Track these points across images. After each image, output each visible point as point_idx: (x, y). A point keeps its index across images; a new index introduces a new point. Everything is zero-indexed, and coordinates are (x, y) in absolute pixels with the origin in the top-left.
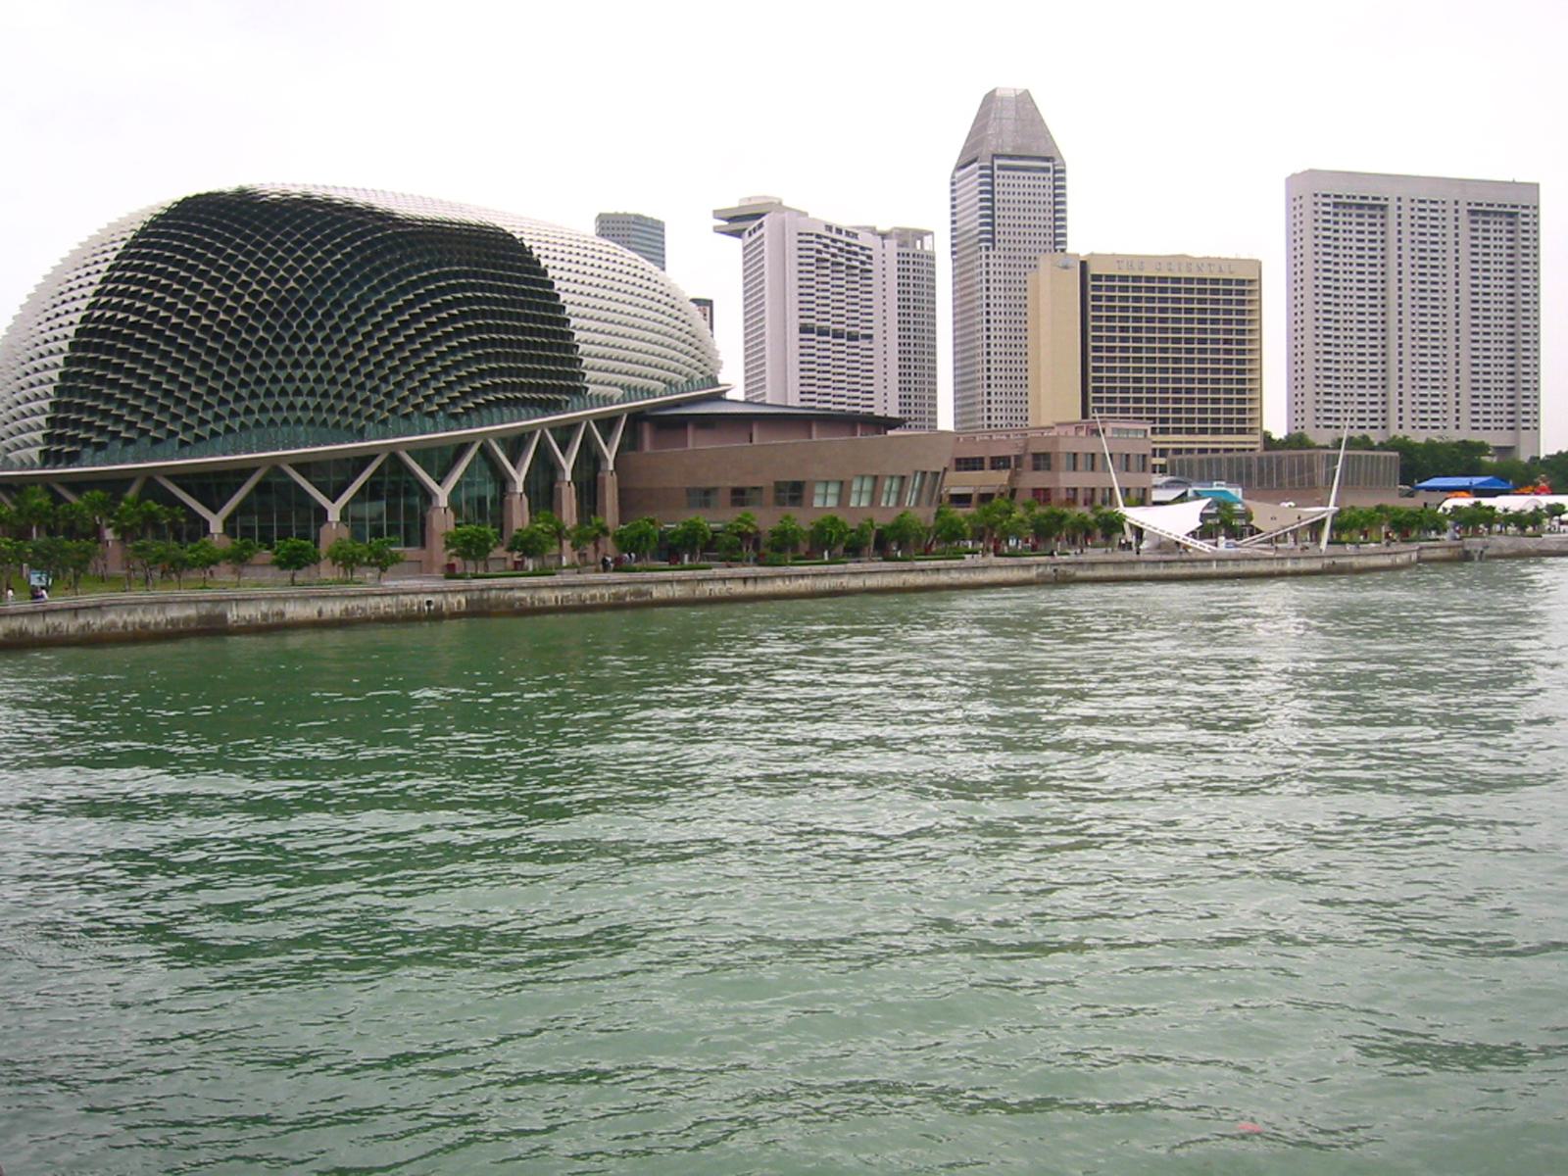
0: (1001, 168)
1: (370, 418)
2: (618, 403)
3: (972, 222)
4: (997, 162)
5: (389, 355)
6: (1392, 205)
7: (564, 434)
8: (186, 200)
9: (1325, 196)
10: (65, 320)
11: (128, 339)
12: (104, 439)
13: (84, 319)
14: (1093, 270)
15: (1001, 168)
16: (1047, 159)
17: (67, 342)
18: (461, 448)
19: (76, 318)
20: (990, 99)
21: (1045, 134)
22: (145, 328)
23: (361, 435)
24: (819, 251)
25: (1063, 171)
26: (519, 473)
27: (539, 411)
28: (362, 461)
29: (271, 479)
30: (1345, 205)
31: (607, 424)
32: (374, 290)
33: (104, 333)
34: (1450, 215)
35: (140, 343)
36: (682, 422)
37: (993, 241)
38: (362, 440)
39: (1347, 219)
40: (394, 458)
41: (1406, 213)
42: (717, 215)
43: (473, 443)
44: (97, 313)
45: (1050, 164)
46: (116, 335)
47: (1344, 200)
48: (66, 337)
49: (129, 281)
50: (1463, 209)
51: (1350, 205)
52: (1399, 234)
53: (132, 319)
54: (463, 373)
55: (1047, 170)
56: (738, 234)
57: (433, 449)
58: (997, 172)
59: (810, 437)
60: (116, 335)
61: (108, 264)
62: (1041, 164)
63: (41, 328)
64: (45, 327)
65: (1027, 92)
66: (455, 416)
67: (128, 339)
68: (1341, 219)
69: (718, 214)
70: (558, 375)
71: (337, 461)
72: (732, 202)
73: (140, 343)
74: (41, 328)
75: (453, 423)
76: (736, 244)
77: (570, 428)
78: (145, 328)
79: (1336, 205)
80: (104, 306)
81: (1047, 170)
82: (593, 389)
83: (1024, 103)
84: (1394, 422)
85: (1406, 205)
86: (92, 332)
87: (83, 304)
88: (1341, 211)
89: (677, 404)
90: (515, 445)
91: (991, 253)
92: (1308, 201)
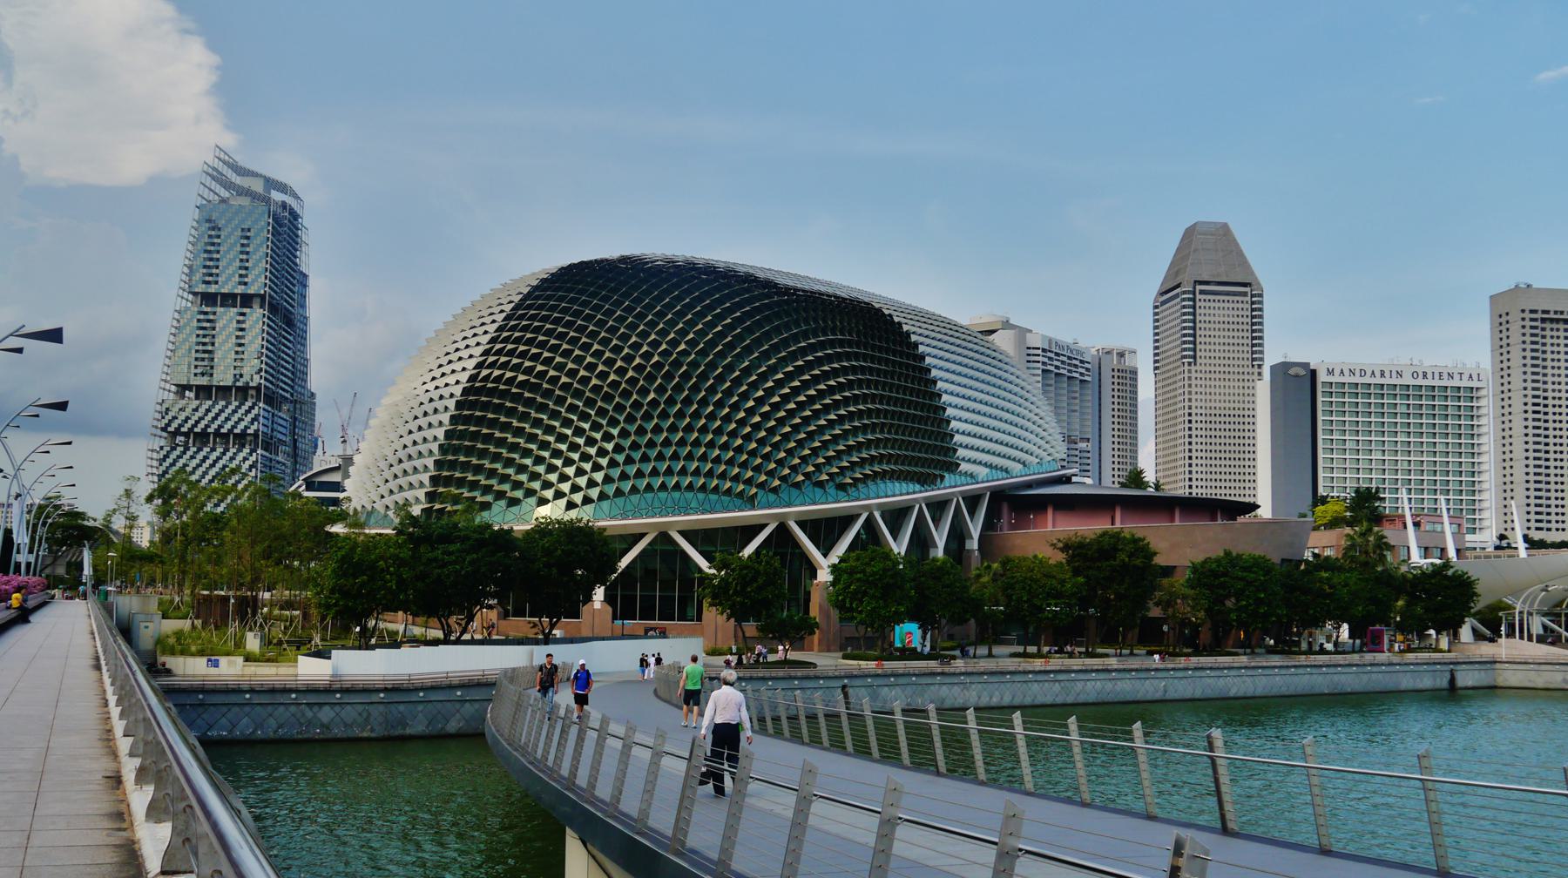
0: (1202, 292)
4: (1199, 287)
5: (781, 422)
7: (938, 507)
8: (571, 266)
9: (1532, 311)
10: (451, 379)
11: (517, 398)
12: (489, 498)
13: (472, 378)
14: (1322, 377)
15: (1202, 292)
16: (1245, 285)
17: (453, 401)
18: (846, 521)
20: (1190, 233)
21: (1244, 263)
23: (751, 502)
24: (1044, 363)
25: (1261, 295)
26: (899, 546)
27: (918, 487)
28: (751, 531)
29: (658, 547)
30: (1552, 320)
31: (973, 501)
32: (766, 355)
33: (492, 392)
35: (529, 403)
37: (1194, 357)
38: (753, 508)
39: (1555, 333)
40: (782, 529)
43: (857, 517)
44: (485, 372)
45: (1248, 289)
46: (504, 394)
47: (1552, 316)
48: (452, 395)
49: (518, 341)
51: (1558, 321)
53: (521, 378)
54: (841, 447)
55: (1245, 294)
58: (1198, 296)
59: (1172, 520)
60: (504, 394)
61: (496, 326)
63: (426, 387)
64: (431, 386)
65: (1225, 226)
67: (517, 398)
68: (1548, 333)
70: (928, 449)
71: (827, 520)
73: (529, 403)
74: (426, 387)
79: (1543, 320)
80: (492, 365)
81: (1245, 294)
82: (964, 467)
86: (479, 391)
87: (471, 364)
88: (1548, 325)
89: (1029, 485)
90: (896, 517)
91: (1193, 368)
92: (1515, 316)
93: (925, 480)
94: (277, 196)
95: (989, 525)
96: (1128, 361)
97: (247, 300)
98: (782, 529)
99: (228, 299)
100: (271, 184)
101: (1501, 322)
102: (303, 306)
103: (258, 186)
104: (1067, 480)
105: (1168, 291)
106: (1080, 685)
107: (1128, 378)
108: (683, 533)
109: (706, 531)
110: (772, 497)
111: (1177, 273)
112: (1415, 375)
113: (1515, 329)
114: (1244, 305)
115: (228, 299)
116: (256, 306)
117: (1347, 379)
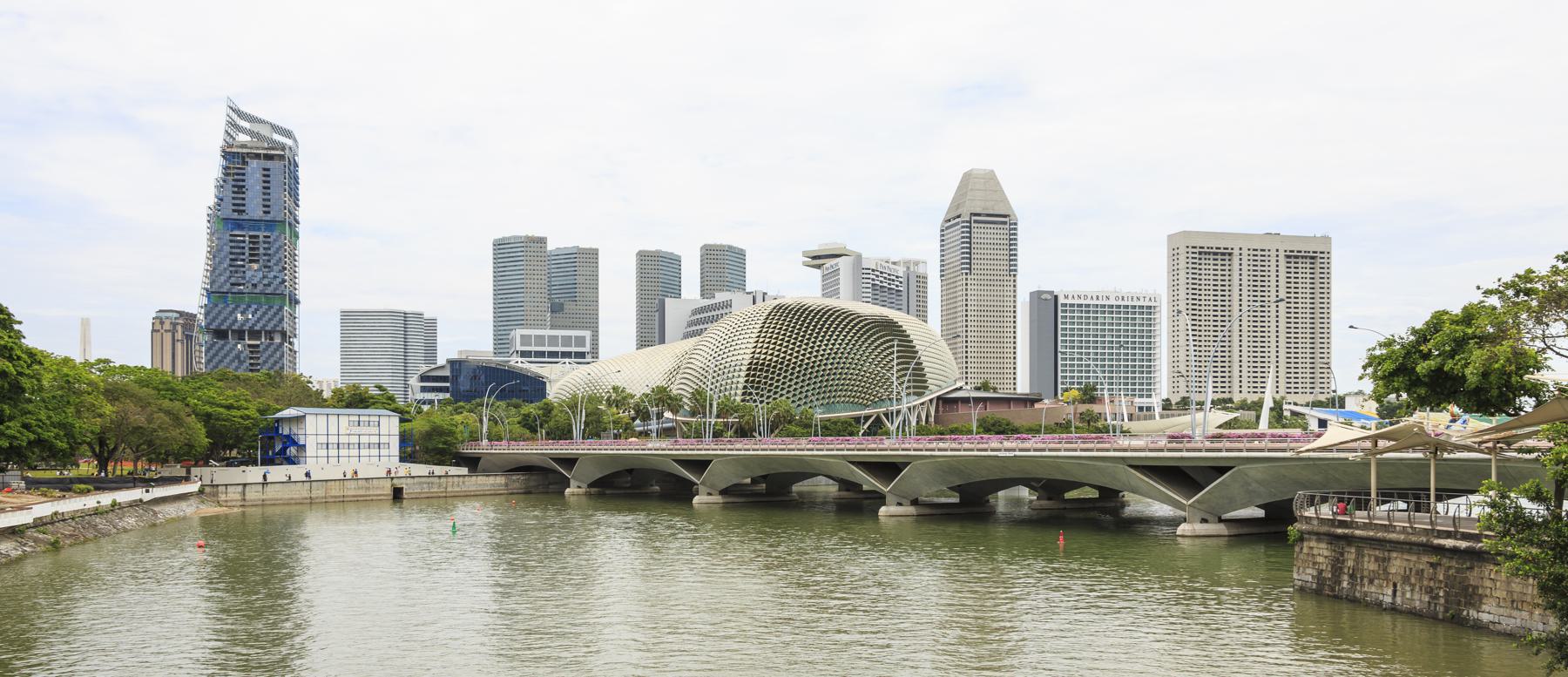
3: (955, 257)
6: (1236, 252)
14: (1061, 300)
20: (967, 178)
21: (1005, 200)
28: (867, 418)
34: (1273, 259)
36: (956, 401)
41: (1245, 258)
42: (805, 254)
50: (1282, 254)
52: (1240, 273)
56: (819, 267)
62: (1003, 220)
69: (805, 254)
72: (815, 247)
76: (818, 272)
83: (990, 179)
84: (1236, 389)
85: (1244, 252)
92: (1182, 250)
95: (937, 411)
96: (921, 270)
98: (878, 419)
101: (1174, 254)
105: (950, 221)
107: (922, 280)
111: (958, 207)
112: (1117, 298)
113: (1182, 258)
114: (1003, 231)
117: (1076, 302)
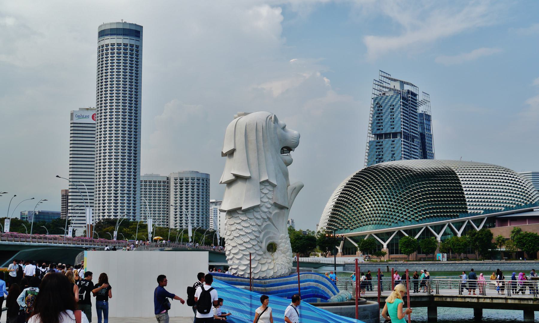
1: (393, 222)
2: (483, 214)
19: (336, 200)
22: (347, 202)
31: (478, 221)
57: (411, 230)
66: (418, 221)
75: (417, 222)
77: (463, 222)
78: (347, 202)
82: (469, 211)
89: (513, 213)
93: (451, 217)
94: (407, 87)
97: (395, 135)
99: (387, 135)
100: (402, 83)
102: (429, 130)
103: (398, 86)
104: (532, 210)
106: (460, 267)
108: (375, 234)
109: (381, 234)
110: (396, 225)
115: (387, 135)
116: (399, 137)
